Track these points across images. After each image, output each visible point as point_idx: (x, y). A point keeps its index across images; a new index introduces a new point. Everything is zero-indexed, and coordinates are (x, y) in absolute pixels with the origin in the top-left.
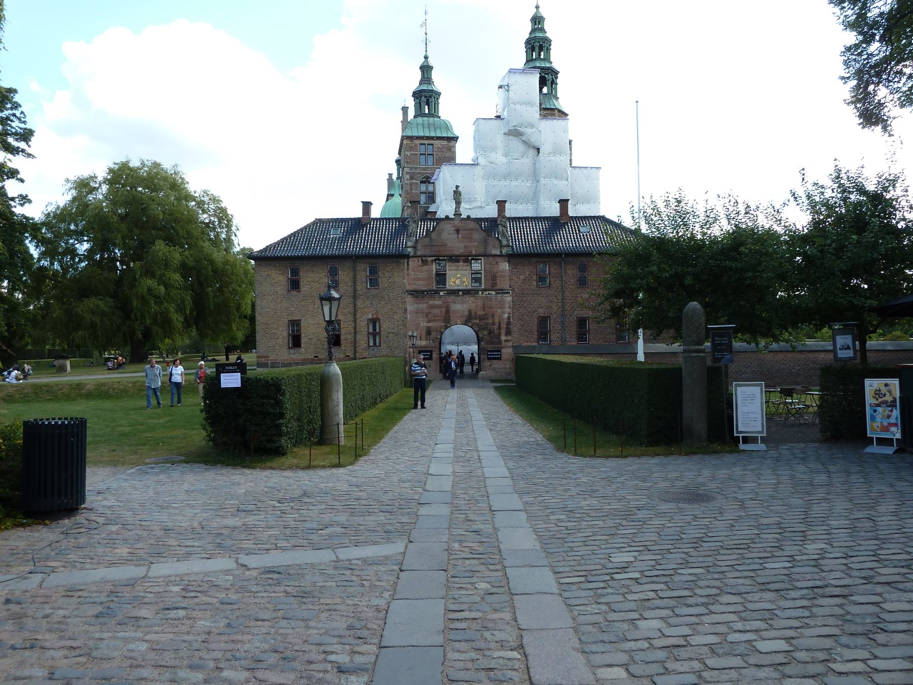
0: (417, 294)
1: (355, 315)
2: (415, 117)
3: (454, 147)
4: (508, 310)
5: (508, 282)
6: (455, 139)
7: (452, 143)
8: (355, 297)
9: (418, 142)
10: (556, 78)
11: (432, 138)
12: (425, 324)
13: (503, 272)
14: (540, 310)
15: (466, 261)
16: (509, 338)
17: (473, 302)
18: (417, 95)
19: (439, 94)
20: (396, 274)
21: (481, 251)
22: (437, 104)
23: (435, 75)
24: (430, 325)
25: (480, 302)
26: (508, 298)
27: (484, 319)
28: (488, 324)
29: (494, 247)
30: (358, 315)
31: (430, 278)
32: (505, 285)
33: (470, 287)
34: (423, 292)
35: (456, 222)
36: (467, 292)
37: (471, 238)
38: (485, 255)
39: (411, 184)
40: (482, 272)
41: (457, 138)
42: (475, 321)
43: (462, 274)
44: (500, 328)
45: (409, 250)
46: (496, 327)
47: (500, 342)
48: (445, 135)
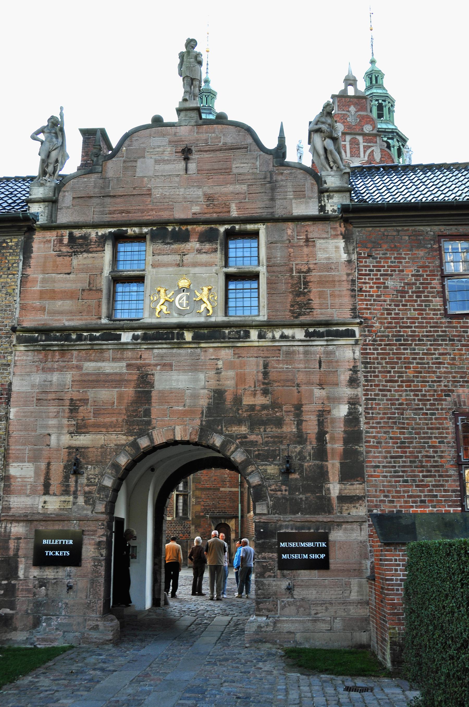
0: (47, 339)
4: (347, 392)
5: (347, 301)
12: (66, 440)
13: (328, 267)
15: (208, 237)
16: (356, 488)
21: (256, 207)
24: (82, 440)
25: (253, 367)
26: (347, 353)
28: (280, 439)
29: (300, 195)
31: (92, 289)
32: (337, 307)
34: (65, 333)
36: (208, 332)
37: (227, 171)
40: (262, 270)
44: (321, 453)
45: (35, 209)
47: (324, 505)
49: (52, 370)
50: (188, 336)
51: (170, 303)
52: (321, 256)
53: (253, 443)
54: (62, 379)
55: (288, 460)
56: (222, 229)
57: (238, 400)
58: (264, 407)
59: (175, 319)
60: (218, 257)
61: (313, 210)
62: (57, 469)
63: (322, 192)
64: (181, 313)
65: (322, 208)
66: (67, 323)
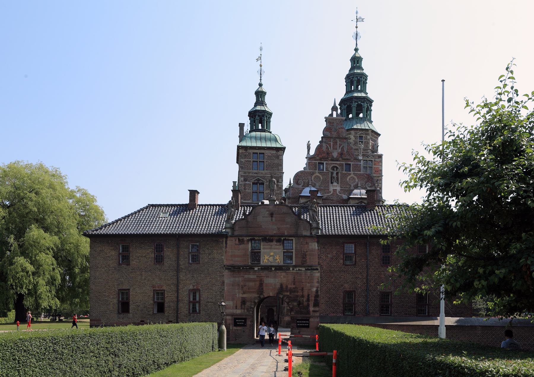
0: (233, 269)
1: (177, 286)
2: (250, 132)
5: (317, 260)
6: (283, 149)
7: (280, 152)
8: (178, 270)
10: (371, 106)
12: (241, 295)
14: (346, 285)
15: (279, 241)
16: (317, 309)
17: (284, 277)
18: (252, 114)
19: (271, 114)
20: (215, 251)
22: (268, 122)
23: (267, 99)
24: (245, 296)
26: (317, 274)
27: (294, 292)
28: (297, 296)
30: (181, 286)
32: (313, 261)
33: (282, 264)
34: (239, 267)
35: (271, 207)
36: (279, 268)
38: (297, 236)
39: (245, 185)
40: (294, 251)
41: (284, 148)
42: (286, 293)
43: (274, 253)
44: (308, 300)
46: (305, 299)
47: (308, 312)
48: (274, 145)
49: (236, 277)
50: (273, 269)
51: (268, 260)
52: (310, 247)
53: (291, 297)
54: (239, 279)
55: (299, 302)
56: (282, 239)
57: (287, 286)
58: (294, 288)
59: (269, 264)
60: (281, 247)
61: (308, 233)
62: (239, 304)
63: (311, 229)
64: (271, 262)
65: (311, 233)
66: (239, 264)
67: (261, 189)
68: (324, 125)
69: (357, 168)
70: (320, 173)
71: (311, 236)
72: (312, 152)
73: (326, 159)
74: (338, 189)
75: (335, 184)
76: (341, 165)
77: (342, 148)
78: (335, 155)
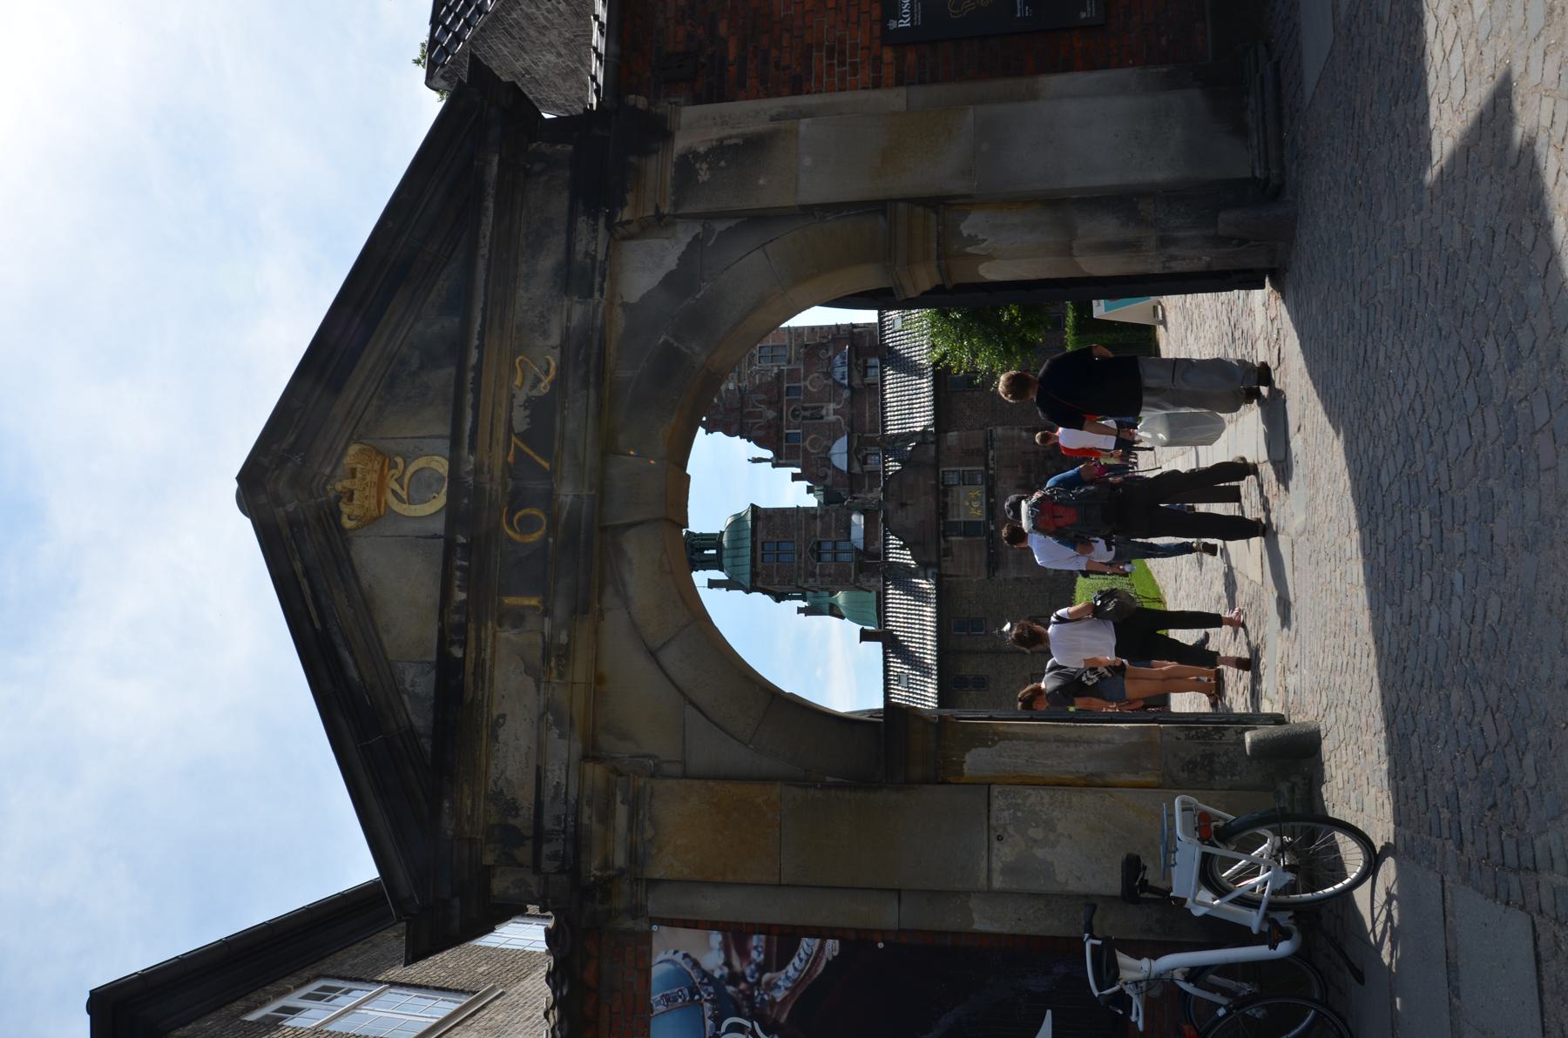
3: (766, 510)
4: (1016, 432)
9: (759, 566)
11: (754, 543)
15: (945, 494)
33: (983, 487)
36: (990, 492)
41: (753, 506)
61: (932, 448)
67: (829, 546)
68: (719, 435)
69: (793, 374)
70: (804, 439)
71: (937, 443)
72: (768, 454)
73: (779, 429)
74: (832, 406)
75: (824, 412)
76: (790, 403)
77: (760, 402)
78: (771, 414)
